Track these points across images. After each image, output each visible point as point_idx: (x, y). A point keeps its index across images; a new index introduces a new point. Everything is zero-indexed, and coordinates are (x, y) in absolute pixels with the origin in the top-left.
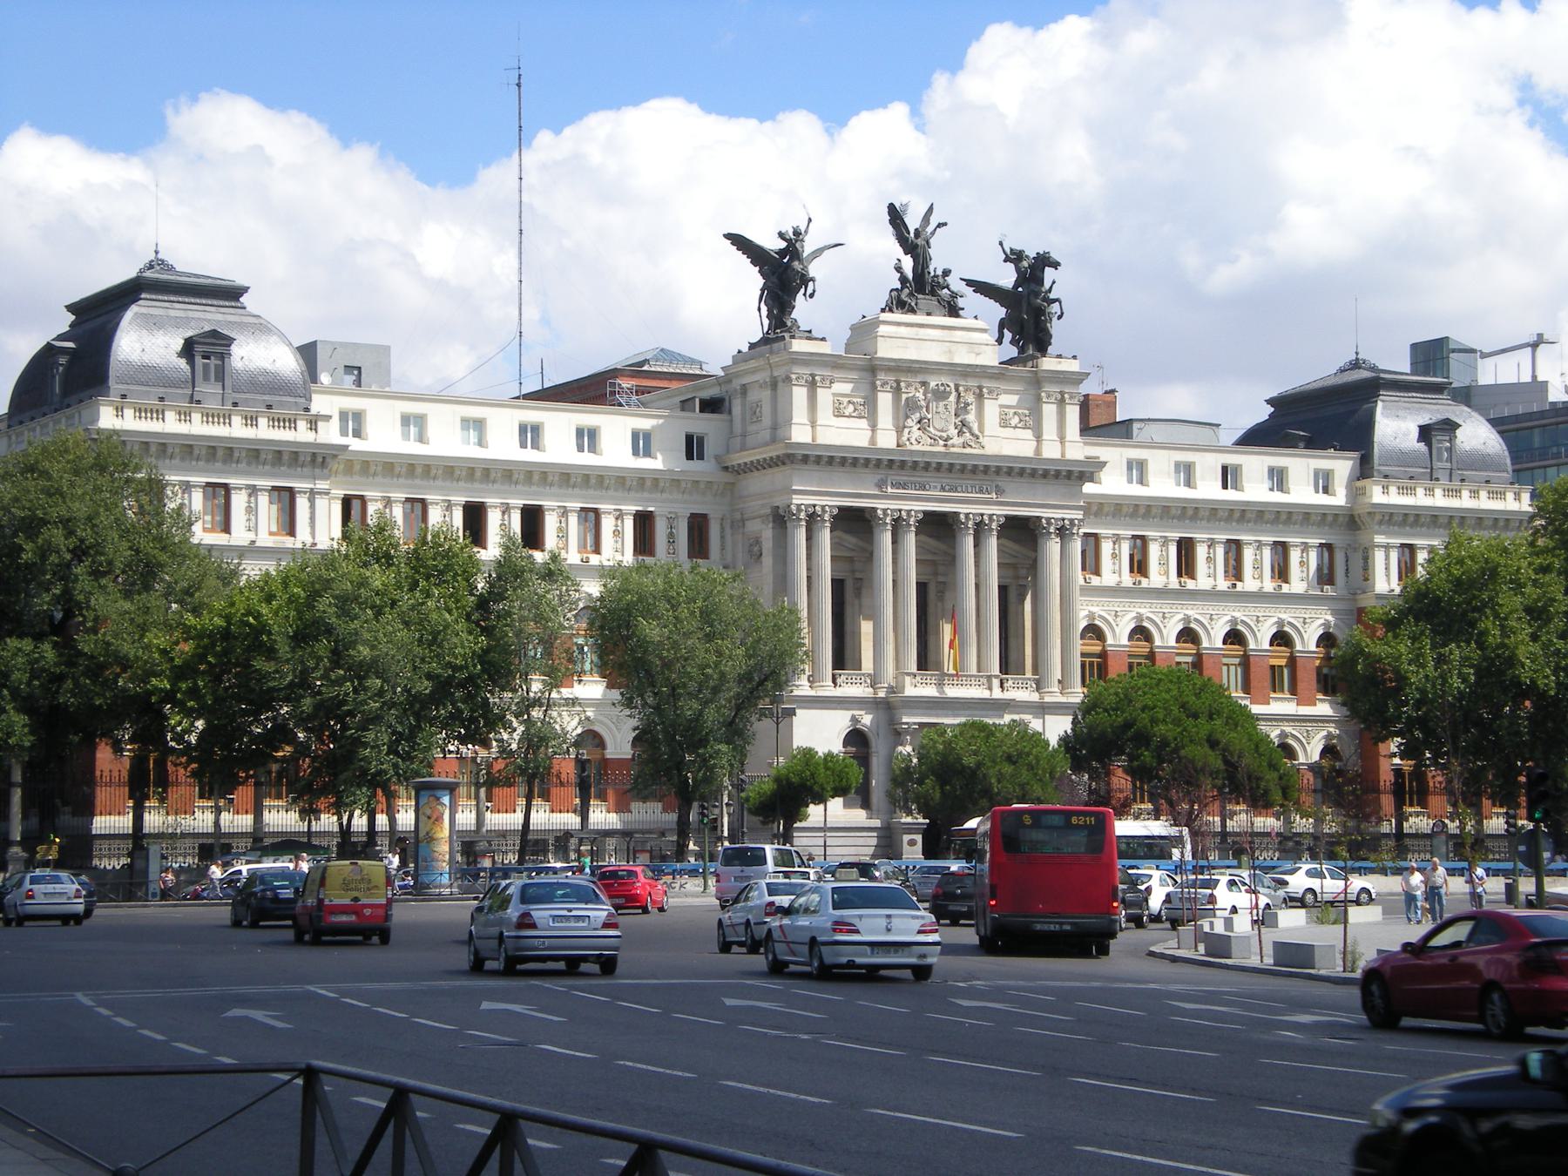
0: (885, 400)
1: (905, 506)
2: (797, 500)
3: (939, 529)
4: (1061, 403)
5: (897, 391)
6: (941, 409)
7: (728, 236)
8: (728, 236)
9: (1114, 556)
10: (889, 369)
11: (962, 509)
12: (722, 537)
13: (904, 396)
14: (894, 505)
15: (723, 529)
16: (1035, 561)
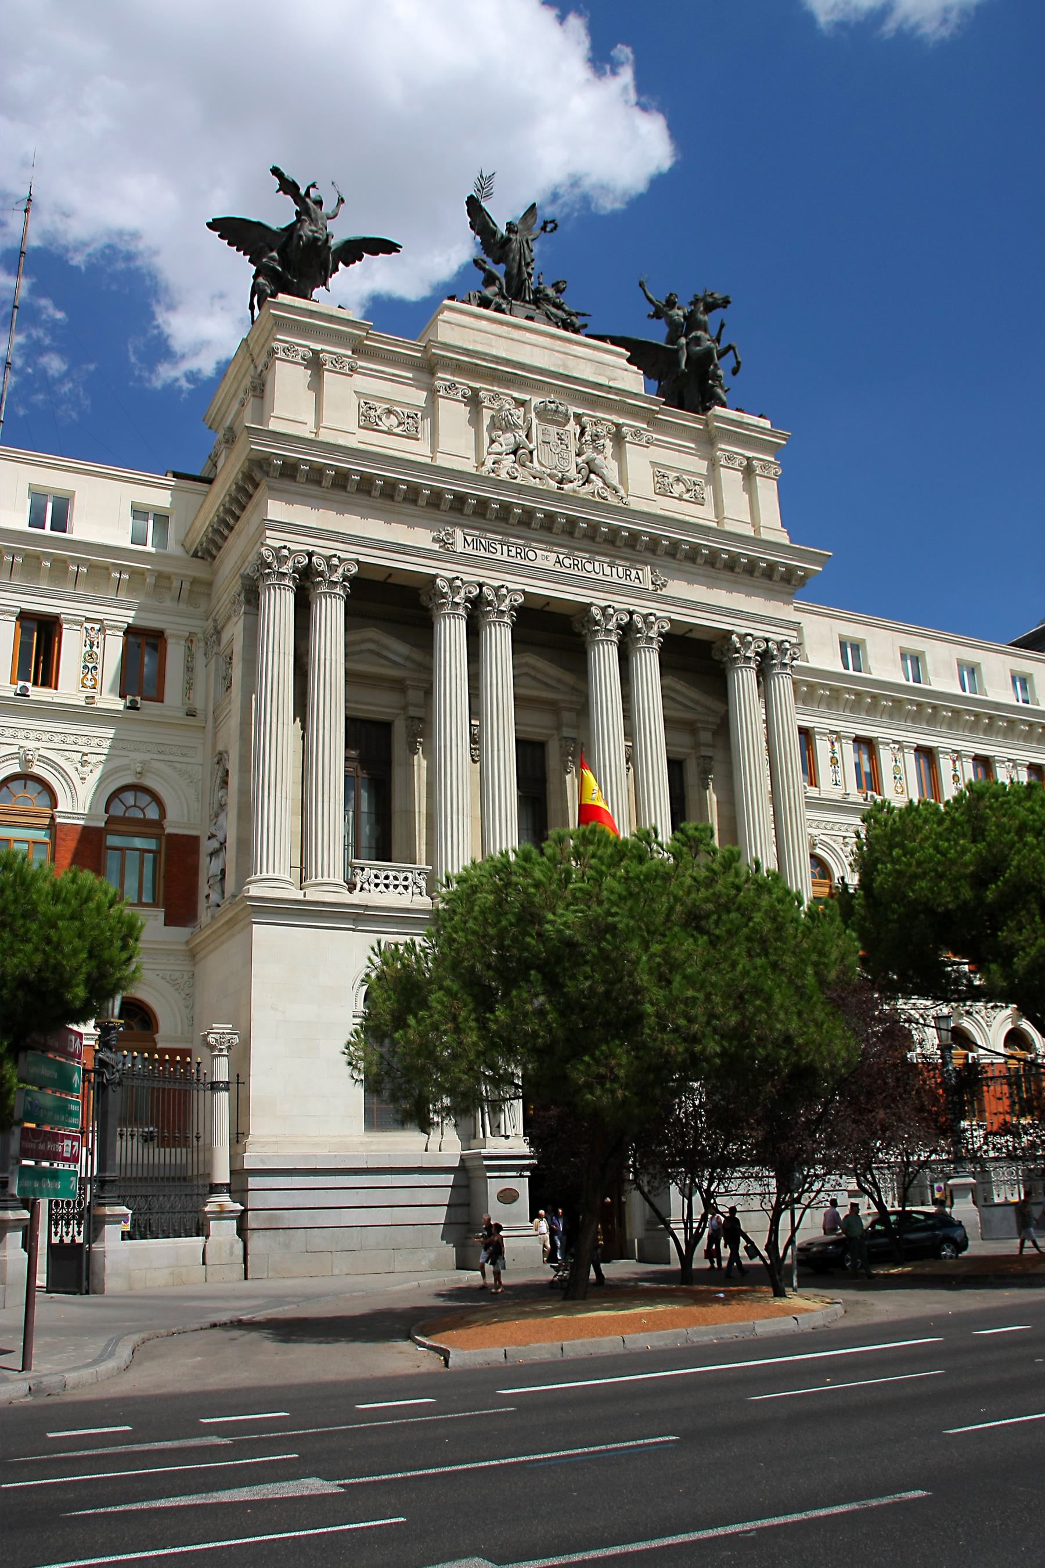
0: (453, 413)
1: (493, 579)
2: (274, 539)
3: (553, 635)
4: (748, 472)
5: (474, 401)
6: (553, 439)
7: (213, 225)
8: (213, 225)
9: (834, 761)
10: (458, 368)
11: (597, 599)
12: (189, 669)
13: (487, 415)
14: (471, 575)
15: (190, 655)
16: (727, 711)
